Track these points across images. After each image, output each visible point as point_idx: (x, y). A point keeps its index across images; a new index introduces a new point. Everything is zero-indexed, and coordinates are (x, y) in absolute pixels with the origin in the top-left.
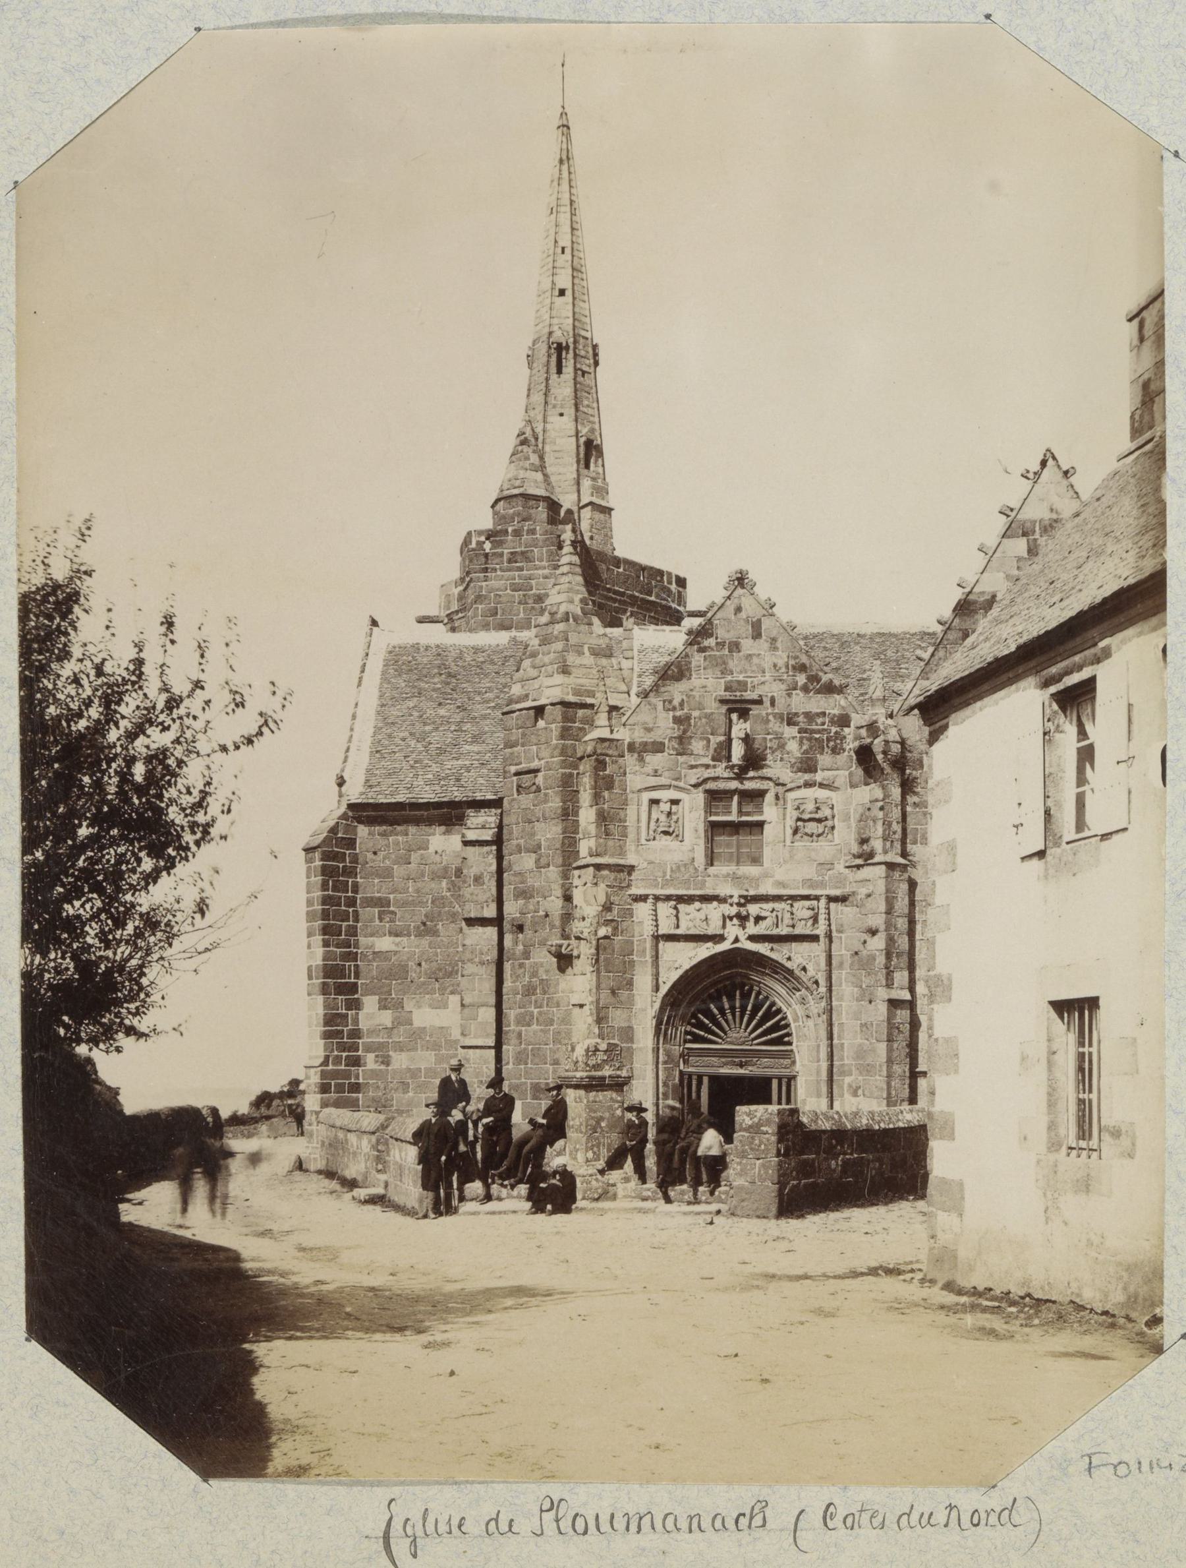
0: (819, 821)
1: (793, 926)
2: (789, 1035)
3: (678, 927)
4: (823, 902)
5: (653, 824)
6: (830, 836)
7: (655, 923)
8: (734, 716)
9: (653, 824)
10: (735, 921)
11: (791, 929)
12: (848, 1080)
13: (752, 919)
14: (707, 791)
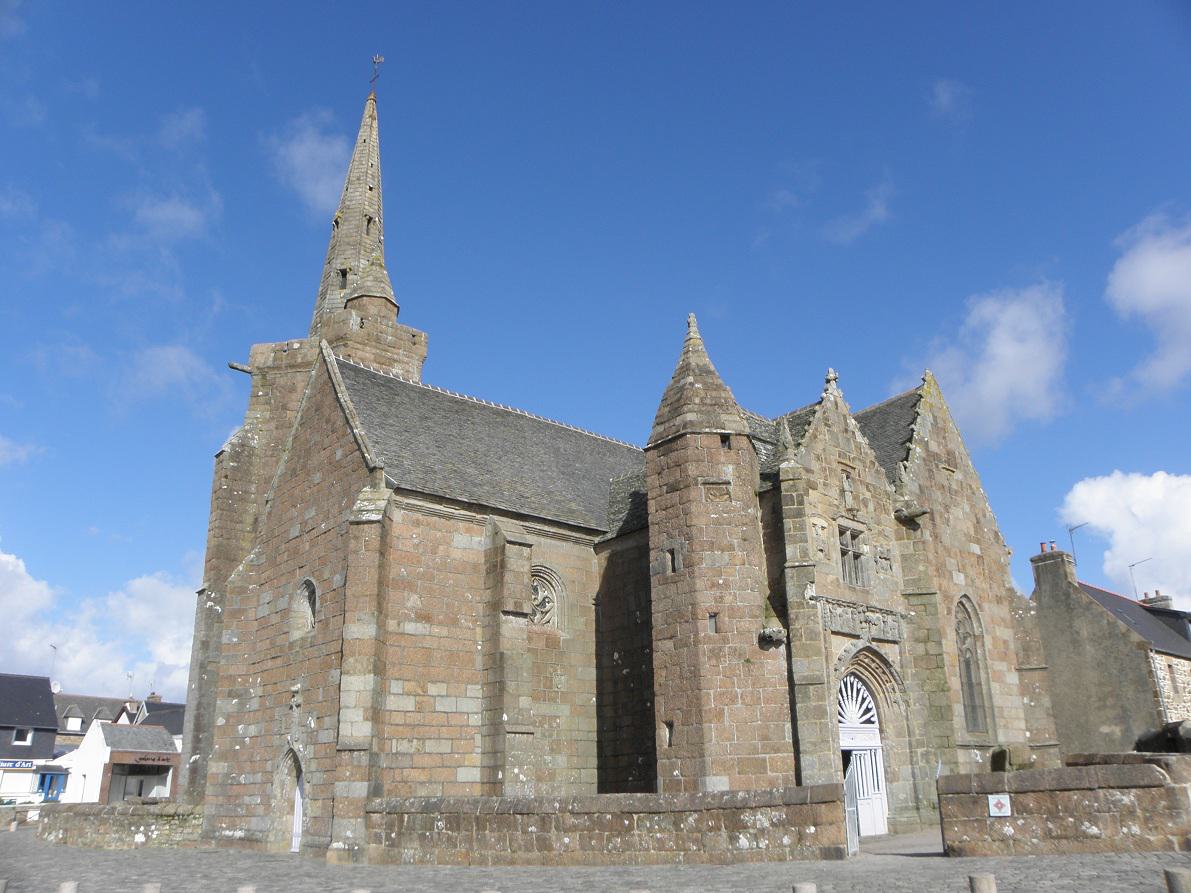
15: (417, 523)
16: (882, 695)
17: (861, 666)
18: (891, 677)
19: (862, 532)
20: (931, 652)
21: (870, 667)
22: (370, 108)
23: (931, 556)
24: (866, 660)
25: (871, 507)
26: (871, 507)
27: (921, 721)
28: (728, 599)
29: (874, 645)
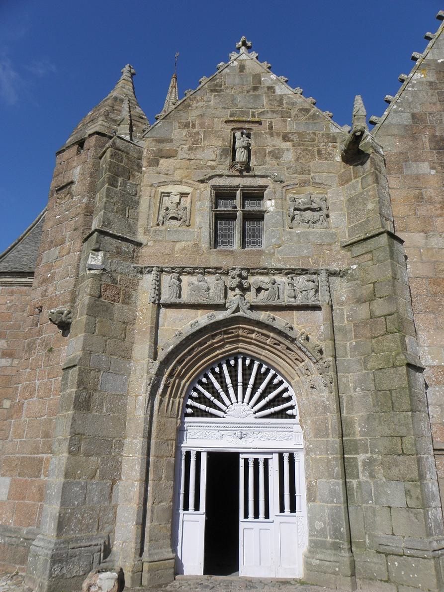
0: (314, 210)
1: (295, 297)
2: (292, 407)
3: (180, 296)
4: (324, 275)
5: (163, 212)
6: (325, 224)
7: (157, 293)
8: (238, 134)
9: (163, 212)
10: (237, 291)
11: (293, 300)
12: (361, 457)
13: (253, 290)
14: (214, 187)
15: (12, 293)
16: (297, 379)
17: (250, 343)
18: (302, 355)
19: (266, 187)
20: (378, 313)
21: (266, 344)
22: (173, 82)
23: (429, 192)
24: (253, 336)
25: (289, 157)
26: (289, 157)
27: (363, 413)
28: (51, 290)
29: (262, 316)
